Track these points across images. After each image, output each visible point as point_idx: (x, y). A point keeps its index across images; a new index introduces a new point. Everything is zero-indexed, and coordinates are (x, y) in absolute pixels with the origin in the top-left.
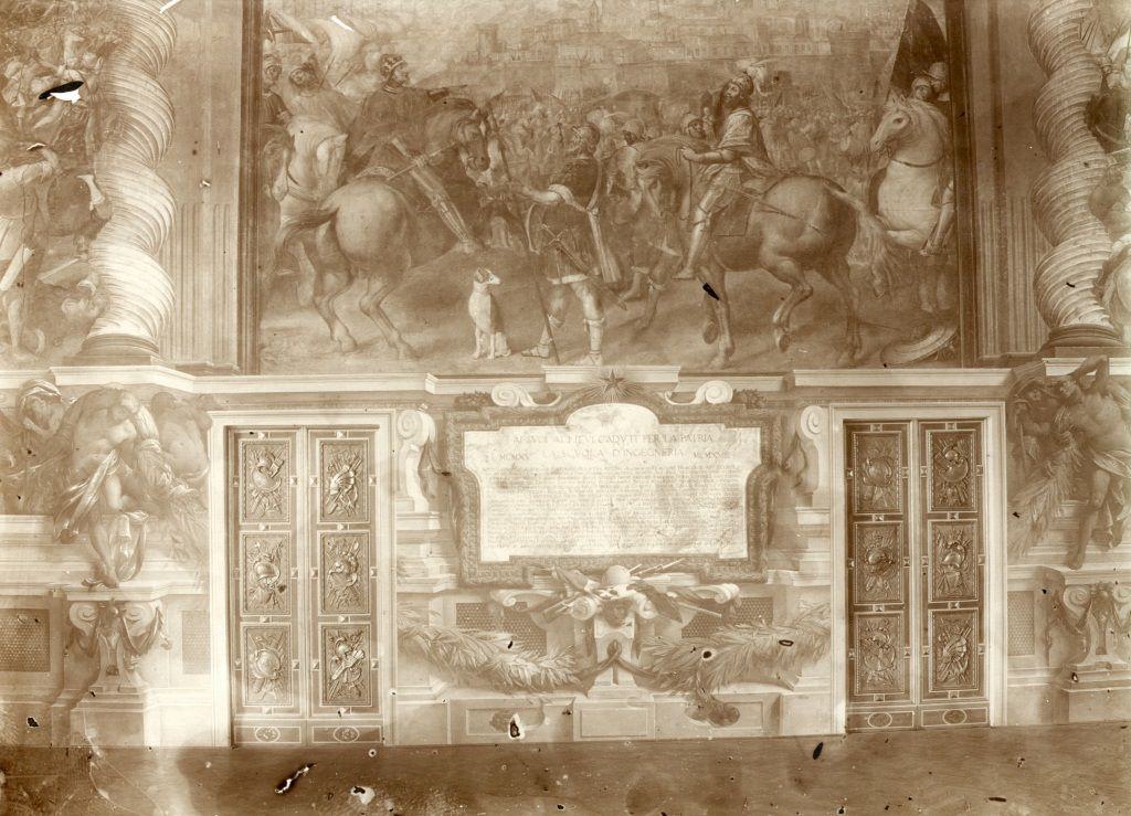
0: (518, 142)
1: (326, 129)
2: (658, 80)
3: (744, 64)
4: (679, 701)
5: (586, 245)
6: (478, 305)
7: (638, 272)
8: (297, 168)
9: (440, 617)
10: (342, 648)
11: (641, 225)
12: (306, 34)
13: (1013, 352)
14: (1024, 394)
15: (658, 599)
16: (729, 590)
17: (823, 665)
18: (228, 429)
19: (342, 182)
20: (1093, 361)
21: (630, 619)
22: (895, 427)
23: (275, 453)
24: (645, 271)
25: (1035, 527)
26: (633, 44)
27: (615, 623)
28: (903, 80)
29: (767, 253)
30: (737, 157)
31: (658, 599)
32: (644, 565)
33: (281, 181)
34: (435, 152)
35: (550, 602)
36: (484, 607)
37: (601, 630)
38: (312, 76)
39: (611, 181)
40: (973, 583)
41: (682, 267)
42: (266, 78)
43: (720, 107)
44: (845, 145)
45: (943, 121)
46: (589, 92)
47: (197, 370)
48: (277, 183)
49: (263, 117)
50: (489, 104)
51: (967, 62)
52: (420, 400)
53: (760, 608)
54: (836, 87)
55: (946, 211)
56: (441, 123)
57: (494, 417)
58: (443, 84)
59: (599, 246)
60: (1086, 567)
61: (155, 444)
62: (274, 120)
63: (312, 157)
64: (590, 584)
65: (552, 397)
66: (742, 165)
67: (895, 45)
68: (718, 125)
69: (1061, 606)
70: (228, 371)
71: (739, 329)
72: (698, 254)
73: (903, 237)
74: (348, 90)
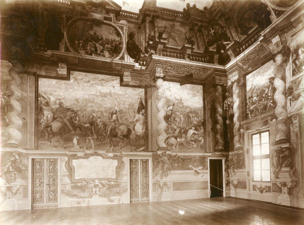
0: (81, 117)
1: (50, 113)
2: (103, 109)
3: (115, 108)
4: (106, 199)
5: (92, 133)
6: (75, 141)
7: (100, 137)
8: (45, 118)
9: (68, 188)
10: (52, 193)
11: (100, 130)
12: (46, 97)
13: (153, 150)
14: (155, 156)
15: (103, 185)
16: (113, 183)
17: (126, 193)
18: (32, 159)
19: (52, 121)
20: (164, 151)
21: (98, 187)
22: (137, 160)
23: (41, 163)
24: (101, 137)
25: (156, 174)
26: (99, 104)
27: (96, 188)
28: (139, 112)
29: (119, 135)
30: (115, 121)
31: (103, 185)
32: (100, 179)
33: (42, 120)
34: (68, 118)
35: (86, 185)
36: (75, 186)
37: (94, 189)
38: (47, 104)
39: (96, 124)
40: (148, 182)
41: (106, 137)
42: (39, 104)
43: (112, 114)
44: (130, 121)
45: (144, 118)
46: (92, 111)
47: (27, 149)
48: (41, 121)
49: (39, 110)
50: (77, 111)
51: (148, 110)
52: (65, 155)
53: (118, 185)
54: (129, 112)
55: (144, 130)
56: (69, 113)
57: (77, 158)
58: (69, 107)
59: (94, 133)
60: (163, 180)
61: (19, 161)
62: (41, 111)
63: (47, 117)
64: (92, 182)
65: (86, 155)
66: (115, 123)
67: (138, 107)
68: (112, 117)
69: (160, 185)
70: (33, 150)
71: (114, 146)
72: (109, 135)
73: (138, 134)
74: (53, 107)
